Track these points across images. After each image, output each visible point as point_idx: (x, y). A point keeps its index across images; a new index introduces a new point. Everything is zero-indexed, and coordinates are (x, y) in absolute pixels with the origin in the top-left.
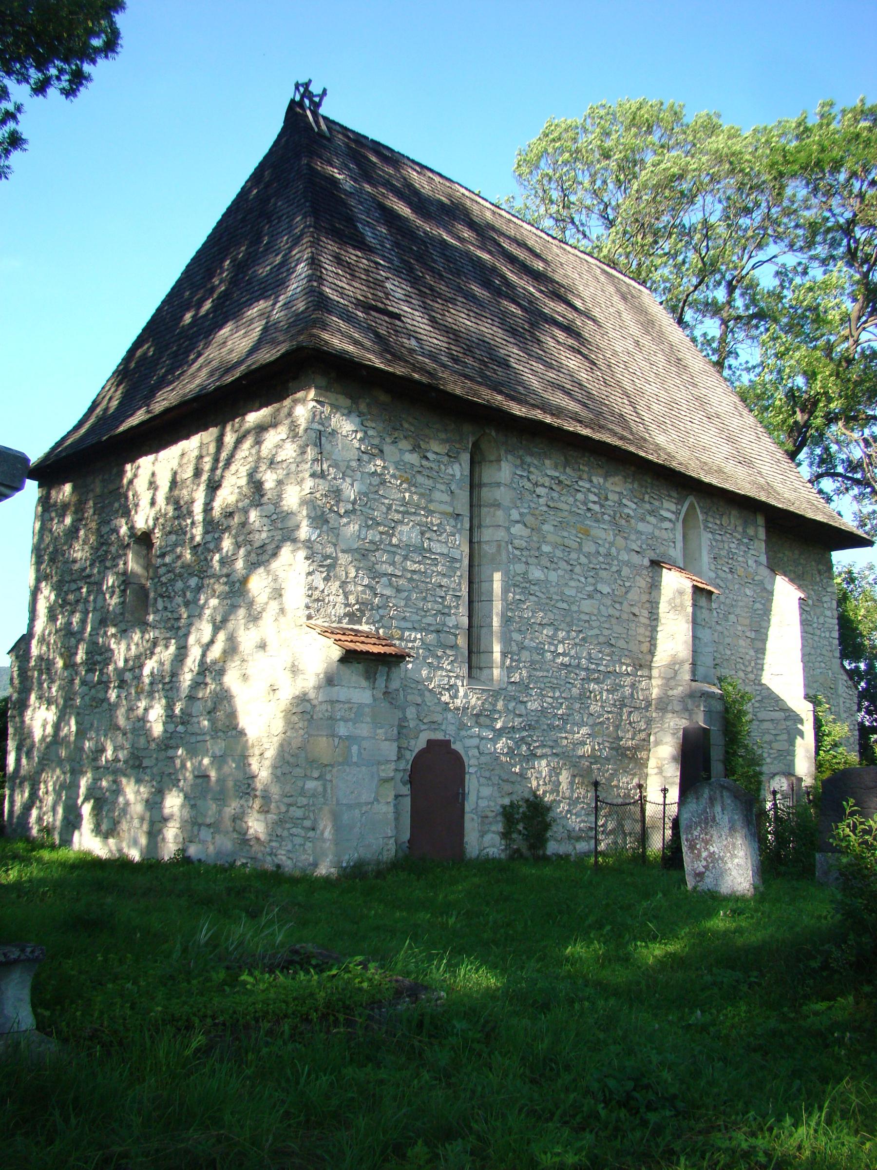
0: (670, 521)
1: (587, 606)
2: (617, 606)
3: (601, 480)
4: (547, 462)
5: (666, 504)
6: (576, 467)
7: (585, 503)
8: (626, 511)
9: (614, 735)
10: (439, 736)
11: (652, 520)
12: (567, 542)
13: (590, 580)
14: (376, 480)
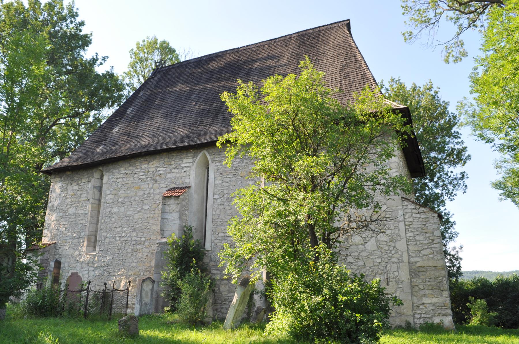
0: (188, 167)
1: (136, 216)
2: (153, 212)
3: (146, 166)
4: (122, 169)
5: (185, 161)
6: (134, 165)
9: (149, 265)
10: (75, 271)
11: (176, 171)
12: (129, 195)
13: (140, 206)
14: (64, 198)
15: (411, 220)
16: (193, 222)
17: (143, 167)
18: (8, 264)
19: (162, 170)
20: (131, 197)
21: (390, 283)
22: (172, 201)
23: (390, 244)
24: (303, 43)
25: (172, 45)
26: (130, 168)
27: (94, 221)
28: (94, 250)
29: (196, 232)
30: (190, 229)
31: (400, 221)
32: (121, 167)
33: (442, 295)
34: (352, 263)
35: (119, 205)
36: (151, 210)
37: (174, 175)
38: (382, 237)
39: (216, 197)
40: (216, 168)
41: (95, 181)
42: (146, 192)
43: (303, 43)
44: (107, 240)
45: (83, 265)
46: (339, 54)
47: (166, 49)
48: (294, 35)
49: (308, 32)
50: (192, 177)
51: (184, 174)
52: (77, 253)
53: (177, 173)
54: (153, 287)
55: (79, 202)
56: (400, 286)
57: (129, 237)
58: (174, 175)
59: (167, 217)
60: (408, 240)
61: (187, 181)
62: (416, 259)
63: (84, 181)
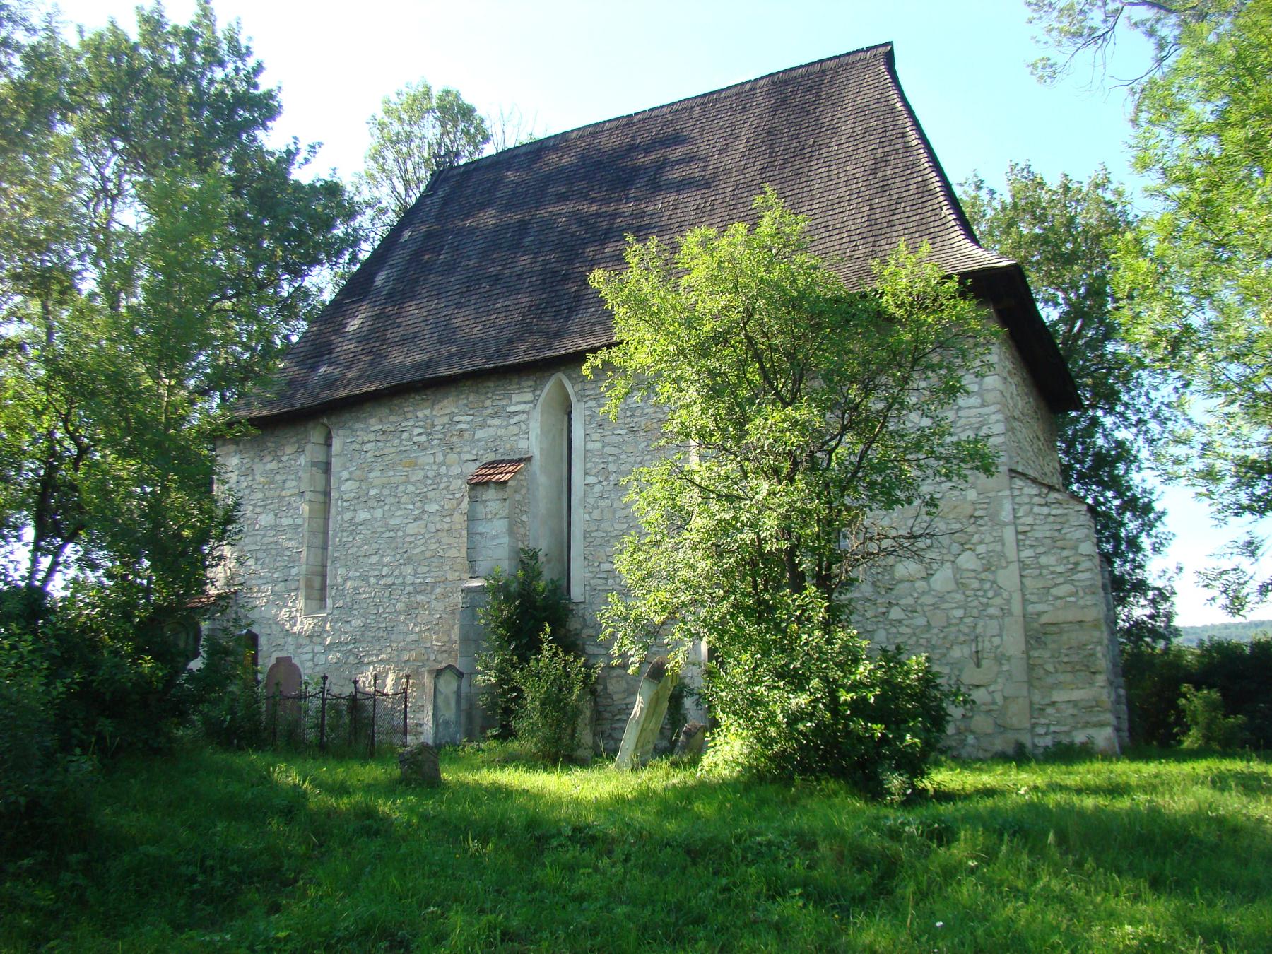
0: (523, 412)
1: (412, 529)
2: (448, 519)
3: (427, 412)
4: (372, 421)
5: (515, 398)
7: (410, 440)
8: (459, 426)
9: (446, 639)
11: (497, 421)
12: (393, 480)
13: (419, 504)
15: (1030, 520)
16: (542, 543)
17: (420, 414)
18: (187, 642)
19: (464, 421)
20: (396, 485)
21: (984, 663)
22: (491, 494)
23: (983, 576)
24: (784, 101)
25: (467, 99)
26: (392, 418)
27: (318, 541)
28: (323, 606)
29: (549, 562)
30: (534, 556)
31: (1006, 524)
32: (371, 416)
33: (1091, 684)
34: (900, 622)
35: (372, 503)
36: (443, 514)
37: (492, 431)
38: (967, 561)
39: (591, 480)
40: (587, 413)
41: (312, 452)
42: (431, 474)
43: (784, 101)
44: (349, 585)
45: (301, 641)
46: (866, 131)
47: (456, 113)
48: (761, 83)
49: (794, 74)
50: (533, 436)
51: (515, 430)
52: (284, 613)
53: (498, 427)
54: (459, 688)
55: (281, 498)
56: (1005, 668)
57: (397, 577)
58: (492, 431)
59: (481, 529)
60: (1023, 566)
61: (523, 444)
62: (1040, 608)
63: (289, 450)
